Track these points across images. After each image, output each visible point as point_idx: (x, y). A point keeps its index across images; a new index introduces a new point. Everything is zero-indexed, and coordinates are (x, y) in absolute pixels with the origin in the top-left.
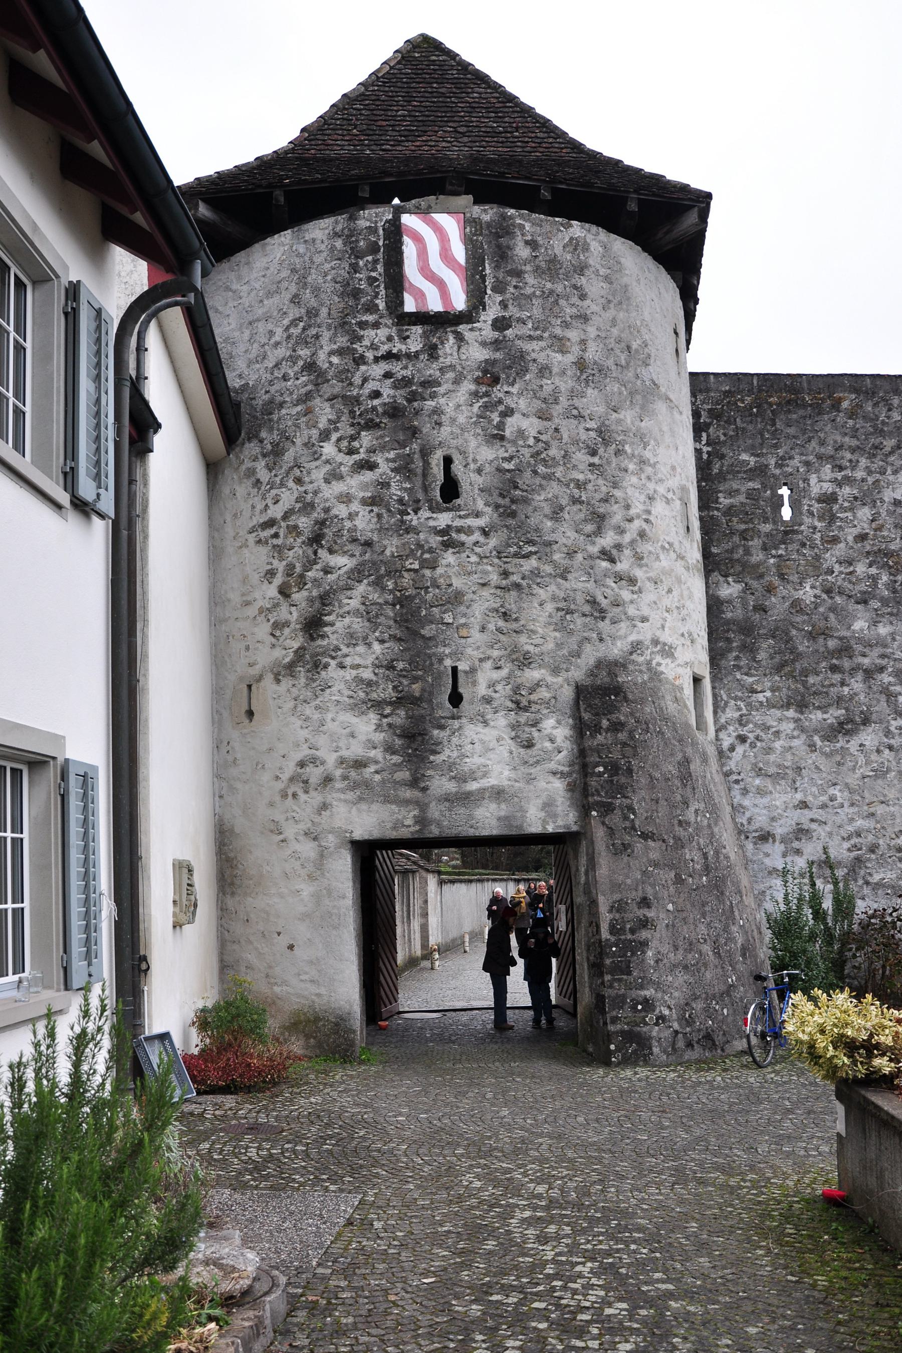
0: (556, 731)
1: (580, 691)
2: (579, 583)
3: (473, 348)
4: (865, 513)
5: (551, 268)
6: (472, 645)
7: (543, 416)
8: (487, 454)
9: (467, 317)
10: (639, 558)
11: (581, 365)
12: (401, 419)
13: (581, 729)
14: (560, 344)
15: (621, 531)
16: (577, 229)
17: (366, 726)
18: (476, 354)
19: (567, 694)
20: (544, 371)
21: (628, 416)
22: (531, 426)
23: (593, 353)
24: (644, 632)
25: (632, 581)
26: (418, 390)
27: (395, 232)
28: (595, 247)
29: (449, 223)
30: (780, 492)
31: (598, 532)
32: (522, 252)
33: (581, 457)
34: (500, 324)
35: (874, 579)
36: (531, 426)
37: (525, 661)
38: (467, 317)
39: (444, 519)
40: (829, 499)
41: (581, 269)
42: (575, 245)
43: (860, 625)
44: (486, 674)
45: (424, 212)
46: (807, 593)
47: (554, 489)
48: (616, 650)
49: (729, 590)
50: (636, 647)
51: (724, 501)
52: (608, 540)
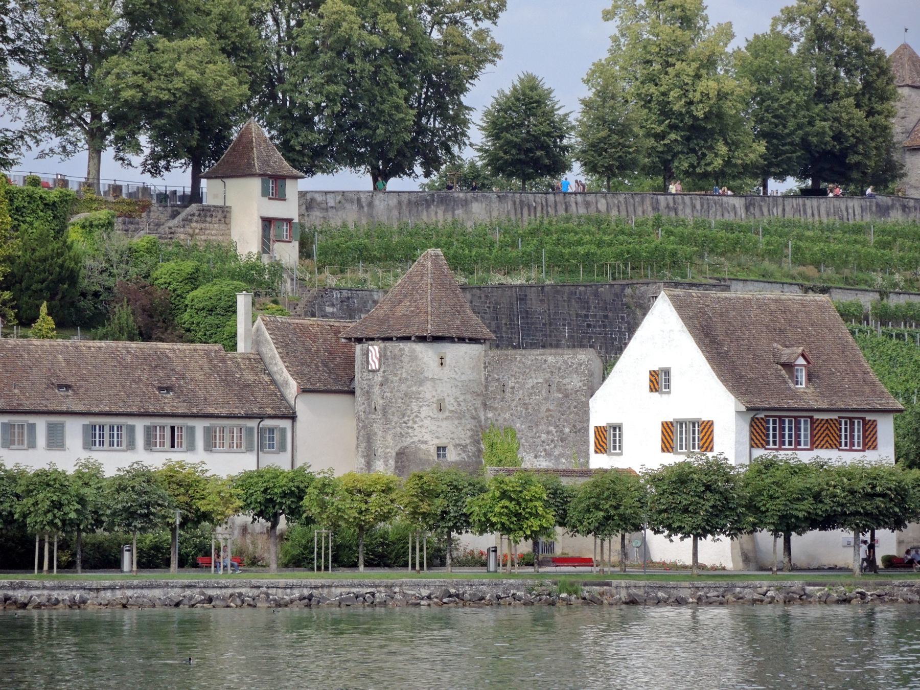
0: (392, 462)
1: (397, 454)
2: (398, 430)
3: (378, 378)
4: (521, 392)
5: (394, 358)
6: (378, 444)
7: (391, 392)
8: (381, 402)
9: (378, 371)
10: (415, 422)
11: (400, 379)
12: (368, 394)
13: (396, 462)
14: (395, 375)
15: (409, 416)
16: (402, 345)
17: (363, 460)
18: (380, 379)
19: (394, 454)
20: (392, 382)
21: (414, 389)
22: (389, 395)
23: (404, 375)
24: (416, 439)
25: (412, 428)
26: (371, 386)
27: (368, 350)
28: (407, 349)
29: (376, 347)
30: (662, 334)
31: (403, 417)
32: (389, 354)
33: (400, 401)
34: (384, 372)
35: (521, 412)
36: (389, 395)
37: (387, 447)
38: (378, 371)
39: (374, 416)
40: (513, 388)
41: (402, 356)
42: (400, 350)
43: (518, 425)
44: (380, 450)
45: (372, 345)
46: (507, 416)
47: (393, 409)
48: (405, 444)
49: (490, 415)
50: (414, 442)
51: (490, 389)
52: (406, 418)
